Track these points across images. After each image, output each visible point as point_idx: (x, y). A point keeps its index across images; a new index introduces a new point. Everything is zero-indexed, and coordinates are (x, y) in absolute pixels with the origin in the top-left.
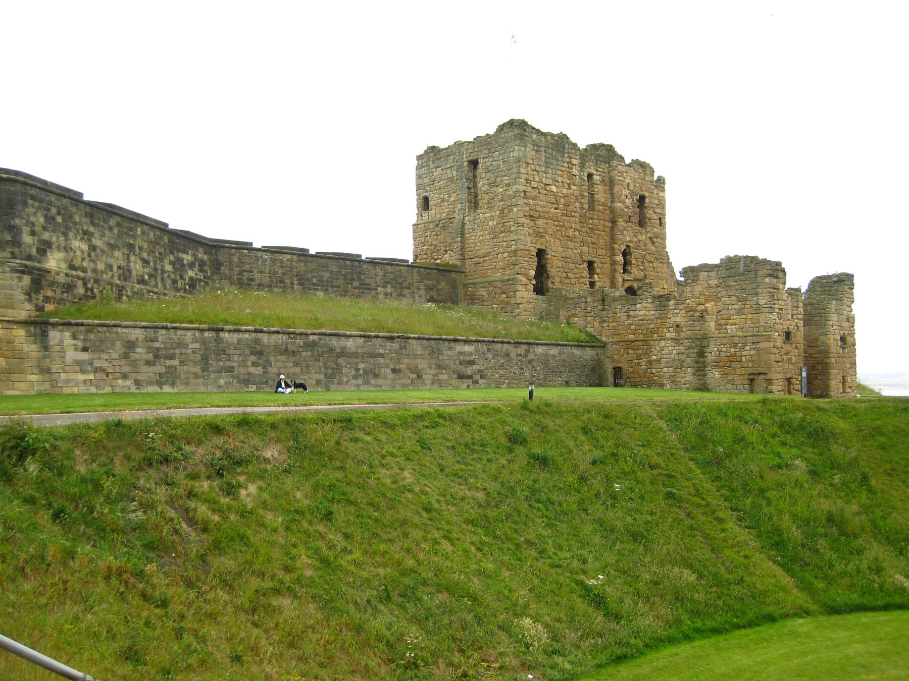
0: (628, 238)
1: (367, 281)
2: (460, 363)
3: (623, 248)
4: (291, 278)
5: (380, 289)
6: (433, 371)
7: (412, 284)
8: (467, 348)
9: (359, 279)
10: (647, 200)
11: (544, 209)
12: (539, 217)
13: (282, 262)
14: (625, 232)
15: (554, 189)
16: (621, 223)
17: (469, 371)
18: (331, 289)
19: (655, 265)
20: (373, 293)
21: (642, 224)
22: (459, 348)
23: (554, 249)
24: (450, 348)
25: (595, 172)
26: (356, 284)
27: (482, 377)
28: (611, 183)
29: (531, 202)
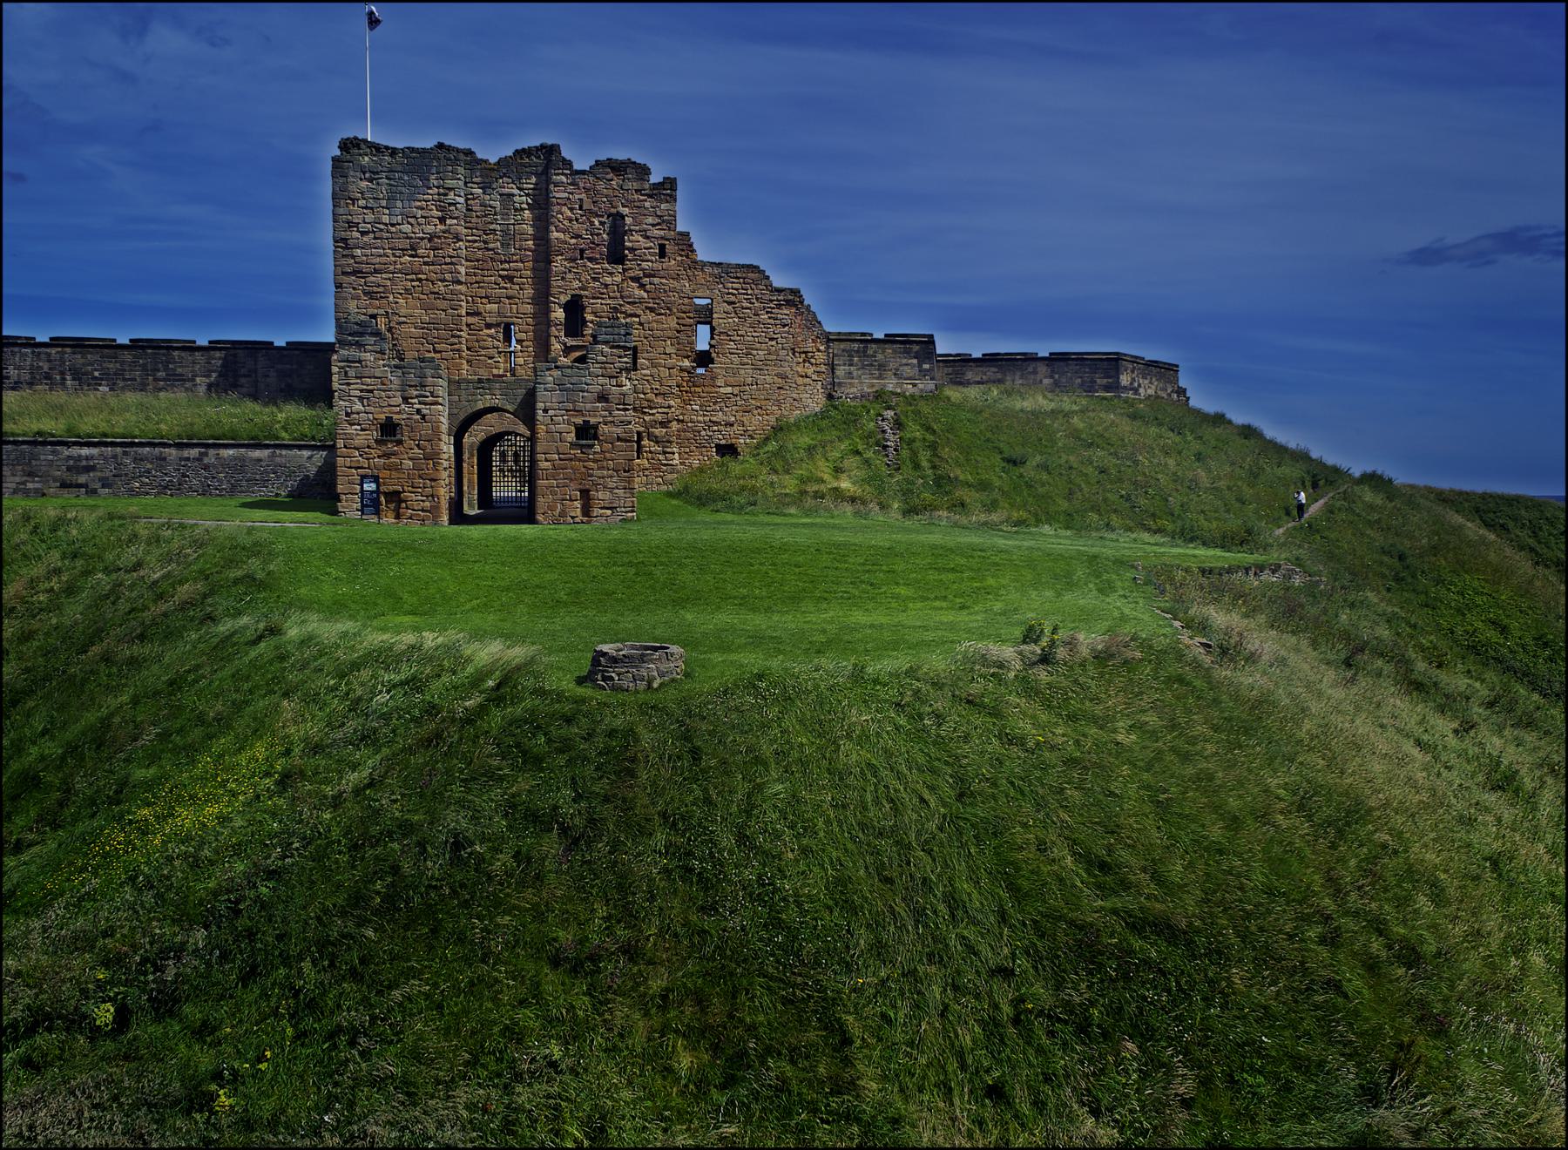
0: (576, 284)
1: (179, 370)
2: (69, 469)
3: (564, 299)
4: (62, 373)
5: (198, 380)
6: (18, 479)
7: (256, 371)
8: (85, 451)
9: (166, 369)
10: (628, 220)
11: (383, 260)
12: (376, 271)
13: (49, 355)
14: (569, 276)
15: (406, 228)
16: (559, 264)
17: (82, 479)
18: (121, 384)
19: (643, 319)
20: (188, 385)
21: (617, 255)
22: (66, 452)
23: (403, 311)
24: (54, 453)
25: (516, 192)
26: (161, 374)
27: (103, 486)
28: (542, 205)
29: (358, 252)
